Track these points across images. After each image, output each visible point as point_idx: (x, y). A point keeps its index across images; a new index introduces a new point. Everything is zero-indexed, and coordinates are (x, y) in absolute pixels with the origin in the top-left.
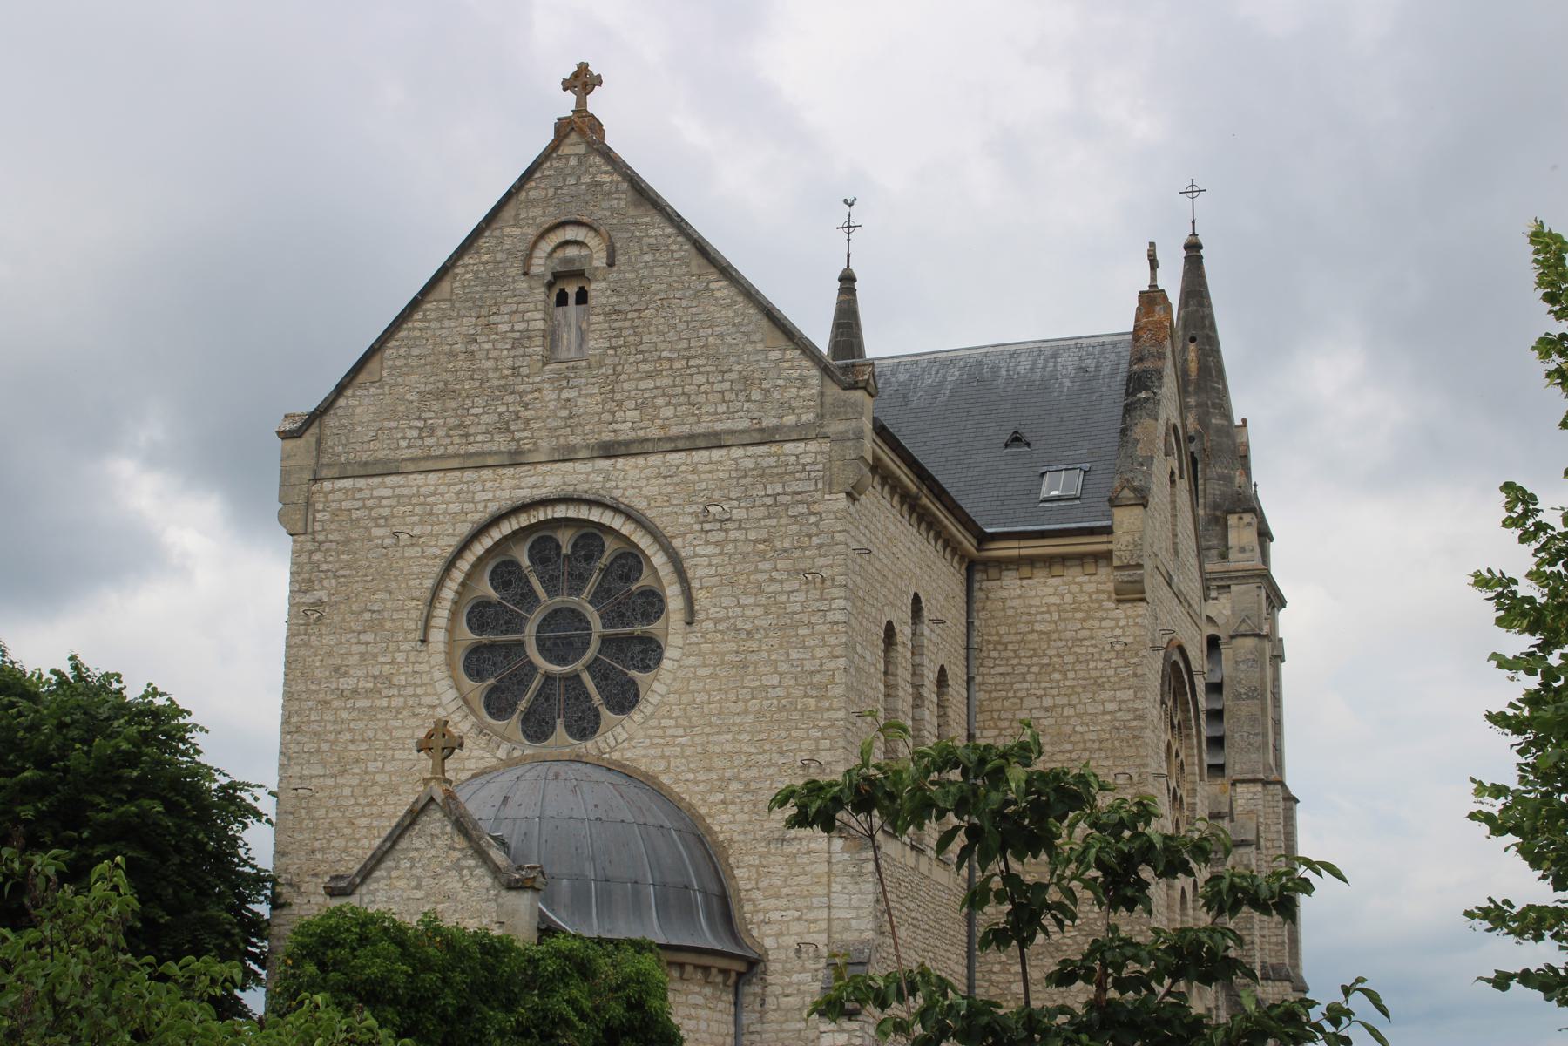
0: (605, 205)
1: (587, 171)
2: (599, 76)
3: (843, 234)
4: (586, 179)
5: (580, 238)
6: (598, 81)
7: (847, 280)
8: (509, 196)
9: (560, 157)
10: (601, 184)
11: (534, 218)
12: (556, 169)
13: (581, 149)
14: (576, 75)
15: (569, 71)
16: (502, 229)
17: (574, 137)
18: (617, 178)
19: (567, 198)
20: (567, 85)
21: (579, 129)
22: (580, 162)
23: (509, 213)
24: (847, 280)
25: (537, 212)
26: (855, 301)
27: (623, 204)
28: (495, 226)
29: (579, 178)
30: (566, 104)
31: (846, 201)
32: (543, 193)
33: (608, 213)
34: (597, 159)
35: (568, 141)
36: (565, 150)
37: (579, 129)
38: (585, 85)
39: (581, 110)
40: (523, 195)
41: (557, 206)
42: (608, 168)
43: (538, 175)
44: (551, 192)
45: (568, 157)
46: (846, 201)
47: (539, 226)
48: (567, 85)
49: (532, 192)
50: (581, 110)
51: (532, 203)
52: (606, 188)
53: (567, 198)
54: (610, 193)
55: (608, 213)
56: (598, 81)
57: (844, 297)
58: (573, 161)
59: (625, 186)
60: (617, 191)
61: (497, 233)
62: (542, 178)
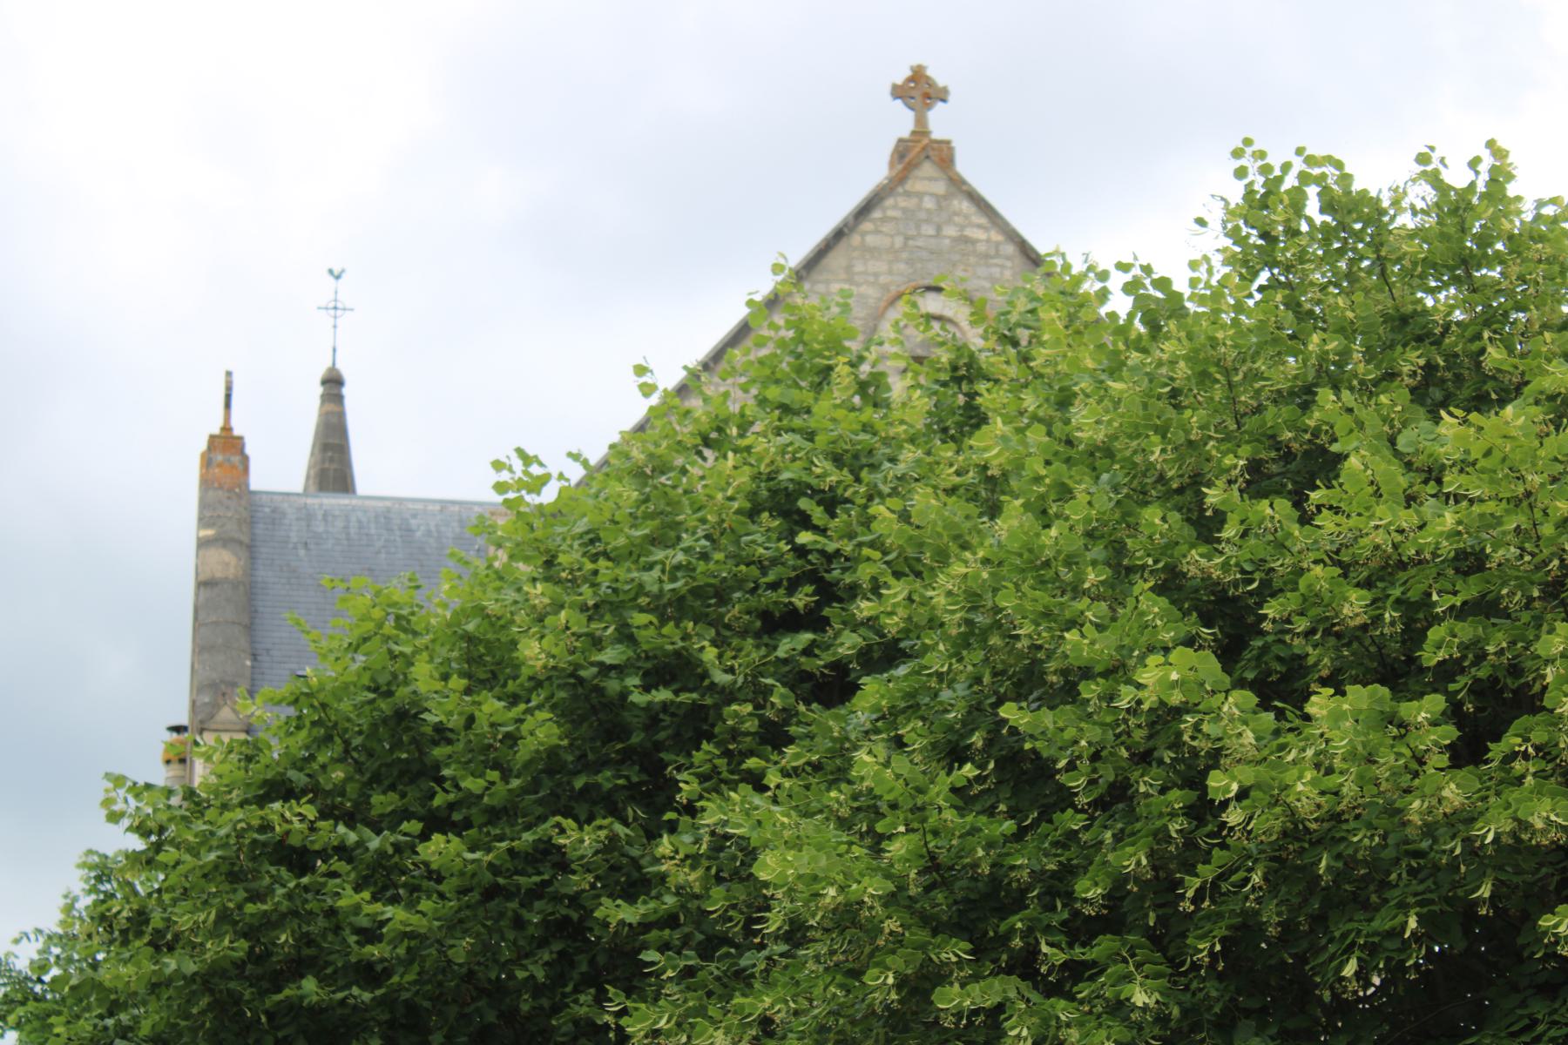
0: (982, 271)
1: (949, 221)
2: (945, 91)
3: (326, 319)
4: (950, 231)
5: (948, 313)
6: (942, 96)
7: (333, 383)
8: (839, 235)
9: (908, 194)
10: (974, 242)
11: (876, 275)
12: (904, 210)
13: (940, 187)
14: (910, 79)
15: (901, 75)
16: (828, 282)
17: (927, 169)
18: (996, 236)
19: (925, 254)
20: (898, 92)
21: (921, 155)
22: (938, 203)
23: (836, 259)
24: (333, 383)
25: (881, 266)
26: (341, 416)
27: (1008, 274)
28: (815, 276)
29: (939, 229)
30: (902, 121)
31: (331, 272)
32: (886, 241)
33: (987, 285)
34: (965, 206)
35: (919, 173)
36: (915, 185)
37: (921, 155)
38: (927, 96)
39: (921, 131)
40: (855, 239)
41: (910, 262)
42: (983, 221)
43: (877, 214)
44: (899, 241)
45: (920, 195)
46: (331, 272)
47: (885, 287)
48: (898, 92)
49: (869, 235)
50: (921, 131)
51: (873, 252)
52: (981, 248)
53: (925, 254)
54: (987, 256)
55: (987, 285)
56: (942, 96)
57: (331, 407)
58: (929, 203)
59: (1010, 249)
60: (997, 255)
61: (821, 288)
62: (884, 220)
